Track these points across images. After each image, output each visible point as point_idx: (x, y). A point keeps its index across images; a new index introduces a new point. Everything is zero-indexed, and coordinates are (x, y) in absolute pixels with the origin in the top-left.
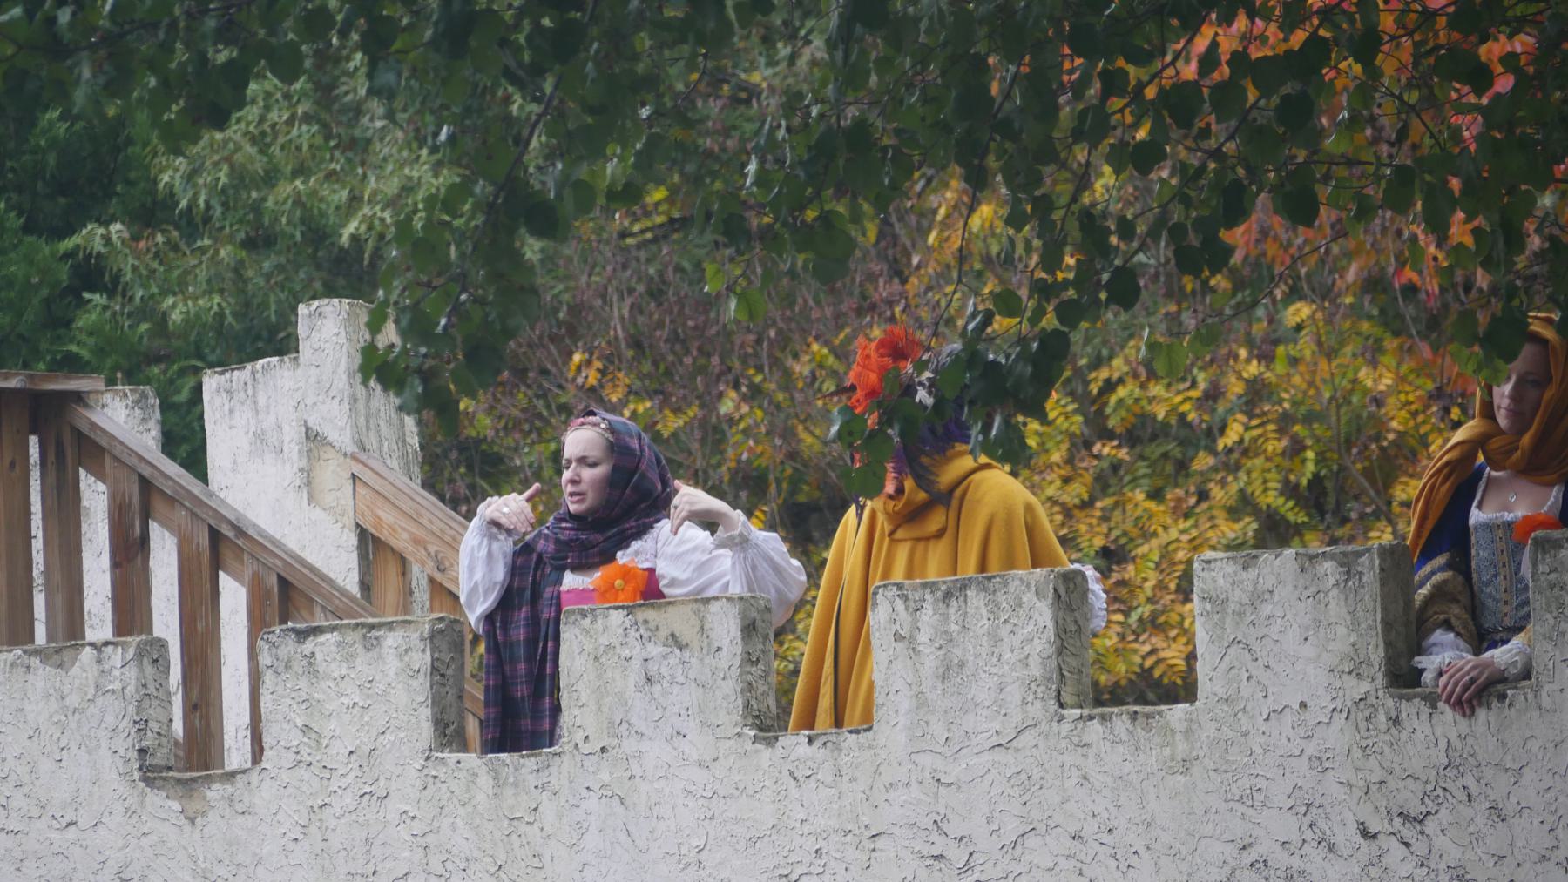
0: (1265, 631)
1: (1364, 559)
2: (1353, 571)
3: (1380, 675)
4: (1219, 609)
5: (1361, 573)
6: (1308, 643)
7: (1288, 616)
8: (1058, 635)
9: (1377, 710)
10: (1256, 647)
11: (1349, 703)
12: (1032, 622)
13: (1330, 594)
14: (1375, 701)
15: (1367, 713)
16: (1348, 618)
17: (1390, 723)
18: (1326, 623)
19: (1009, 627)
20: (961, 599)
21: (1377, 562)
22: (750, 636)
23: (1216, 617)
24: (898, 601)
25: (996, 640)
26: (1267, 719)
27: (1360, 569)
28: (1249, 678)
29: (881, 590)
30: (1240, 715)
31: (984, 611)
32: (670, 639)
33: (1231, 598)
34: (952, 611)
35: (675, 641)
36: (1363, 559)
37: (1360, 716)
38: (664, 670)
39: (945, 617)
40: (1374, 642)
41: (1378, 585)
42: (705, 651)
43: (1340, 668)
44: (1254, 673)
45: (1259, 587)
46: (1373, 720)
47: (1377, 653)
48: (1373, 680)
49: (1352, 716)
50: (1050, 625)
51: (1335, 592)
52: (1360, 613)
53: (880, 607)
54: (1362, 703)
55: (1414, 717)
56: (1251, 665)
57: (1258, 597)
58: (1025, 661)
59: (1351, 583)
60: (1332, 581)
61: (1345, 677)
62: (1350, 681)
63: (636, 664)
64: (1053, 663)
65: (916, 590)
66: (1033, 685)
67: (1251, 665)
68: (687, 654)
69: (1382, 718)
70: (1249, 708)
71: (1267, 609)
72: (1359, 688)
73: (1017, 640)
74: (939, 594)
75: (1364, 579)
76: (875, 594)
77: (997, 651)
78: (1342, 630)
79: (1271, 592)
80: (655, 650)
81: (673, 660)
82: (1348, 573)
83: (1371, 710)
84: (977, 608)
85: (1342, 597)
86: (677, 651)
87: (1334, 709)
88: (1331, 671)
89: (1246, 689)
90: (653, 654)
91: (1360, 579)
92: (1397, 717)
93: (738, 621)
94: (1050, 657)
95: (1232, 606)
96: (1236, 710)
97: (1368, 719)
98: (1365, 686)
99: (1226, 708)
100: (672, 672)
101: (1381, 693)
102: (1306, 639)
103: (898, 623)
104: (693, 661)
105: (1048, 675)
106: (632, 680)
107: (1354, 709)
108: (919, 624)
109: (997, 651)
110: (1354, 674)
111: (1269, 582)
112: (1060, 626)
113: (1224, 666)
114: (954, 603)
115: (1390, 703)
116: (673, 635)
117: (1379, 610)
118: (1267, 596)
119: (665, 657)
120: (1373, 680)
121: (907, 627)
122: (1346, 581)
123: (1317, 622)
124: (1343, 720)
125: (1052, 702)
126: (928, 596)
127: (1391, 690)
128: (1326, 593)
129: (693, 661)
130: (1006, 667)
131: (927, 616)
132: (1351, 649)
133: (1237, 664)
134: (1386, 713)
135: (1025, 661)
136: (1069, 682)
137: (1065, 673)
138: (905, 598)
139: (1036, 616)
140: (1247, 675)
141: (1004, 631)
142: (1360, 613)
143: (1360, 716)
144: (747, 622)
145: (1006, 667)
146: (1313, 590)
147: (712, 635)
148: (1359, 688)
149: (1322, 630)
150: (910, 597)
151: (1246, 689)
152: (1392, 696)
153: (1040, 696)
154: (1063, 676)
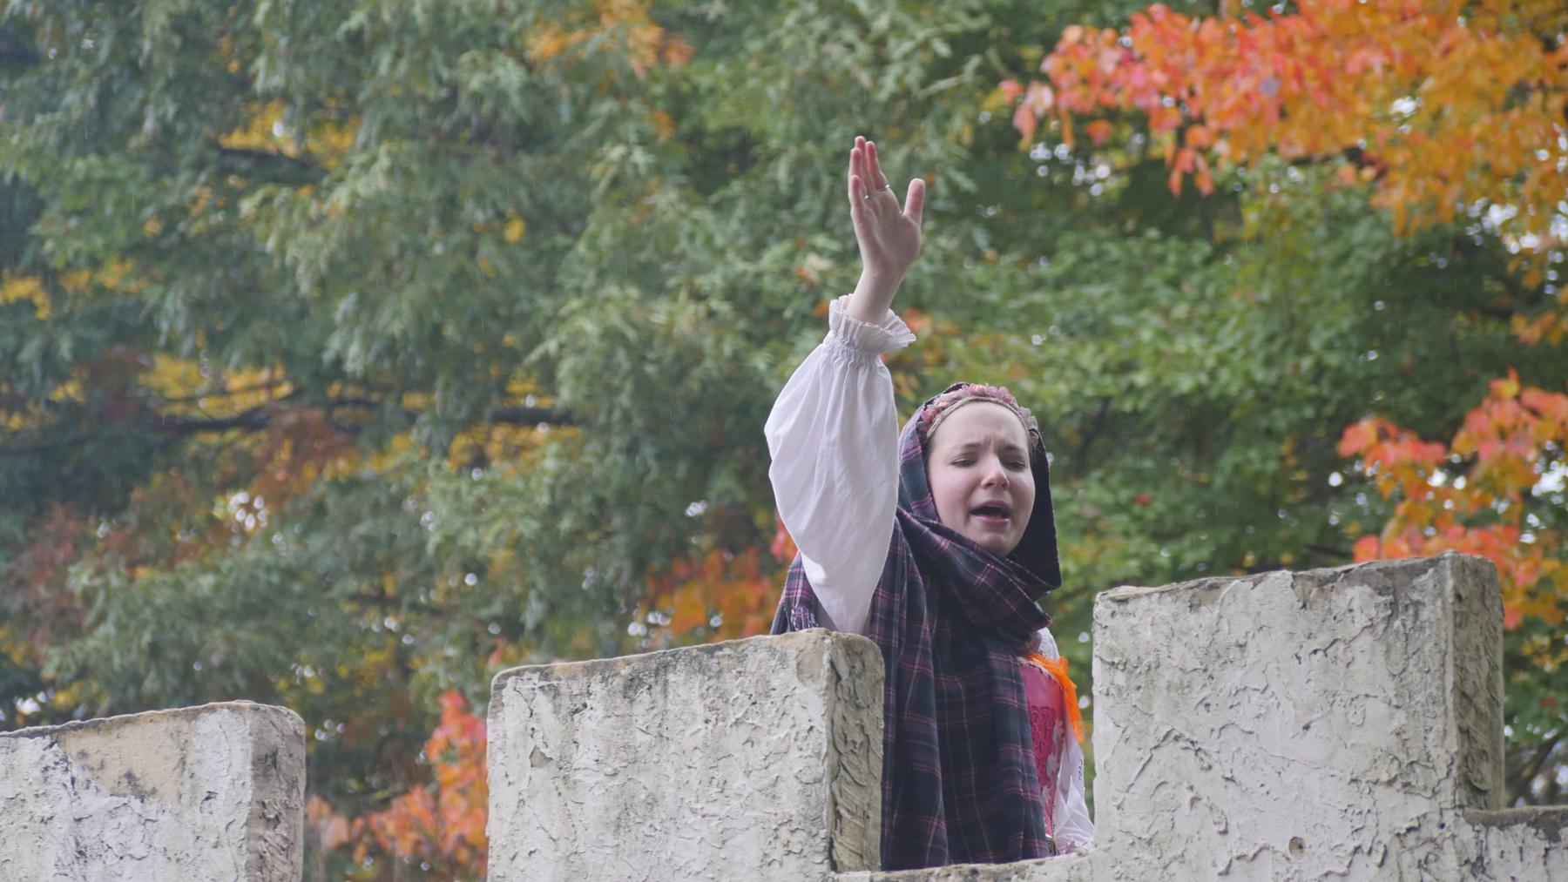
0: (1230, 715)
1: (1427, 579)
2: (1403, 601)
3: (1448, 785)
4: (1141, 681)
5: (1417, 604)
6: (1312, 731)
7: (1273, 688)
8: (833, 744)
9: (1440, 848)
10: (1210, 745)
11: (1386, 838)
12: (787, 721)
13: (1356, 645)
14: (1436, 832)
15: (1421, 854)
16: (1391, 685)
17: (1466, 869)
18: (1346, 697)
19: (743, 732)
20: (658, 688)
21: (1450, 583)
22: (266, 775)
23: (1135, 696)
24: (541, 698)
25: (717, 755)
26: (1226, 872)
27: (1415, 596)
28: (1194, 800)
29: (510, 681)
30: (1174, 867)
31: (699, 708)
32: (125, 782)
33: (1165, 661)
34: (639, 709)
35: (133, 784)
36: (1424, 577)
37: (1407, 858)
38: (110, 837)
39: (627, 721)
40: (1438, 725)
41: (1450, 623)
42: (185, 800)
43: (1372, 776)
44: (1203, 792)
45: (1219, 638)
46: (1433, 866)
47: (1444, 748)
48: (1435, 793)
49: (1391, 861)
50: (821, 725)
51: (1366, 640)
52: (1414, 676)
53: (507, 709)
54: (1412, 835)
55: (1514, 856)
56: (1198, 779)
57: (1215, 658)
58: (770, 792)
59: (1397, 623)
60: (1361, 620)
61: (1380, 791)
62: (1390, 799)
63: (61, 827)
64: (824, 792)
65: (574, 678)
66: (784, 833)
67: (1198, 779)
68: (152, 806)
69: (1450, 860)
70: (1188, 856)
71: (1232, 677)
72: (1402, 810)
73: (756, 755)
74: (618, 682)
75: (1425, 614)
76: (500, 687)
77: (719, 775)
78: (1376, 709)
79: (1242, 646)
80: (95, 802)
81: (126, 819)
82: (1393, 605)
83: (1429, 847)
84: (685, 702)
85: (1381, 648)
86: (136, 803)
87: (1357, 849)
88: (1354, 781)
89: (1186, 821)
90: (90, 811)
91: (1416, 615)
92: (1480, 858)
93: (249, 746)
94: (818, 781)
95: (1167, 675)
96: (1167, 857)
97: (1423, 865)
98: (1419, 806)
99: (1147, 857)
100: (123, 839)
101: (1449, 817)
102: (1307, 727)
103: (538, 735)
104: (162, 818)
105: (812, 813)
106: (50, 857)
107: (1395, 847)
108: (578, 736)
109: (719, 775)
110: (1398, 785)
111: (1240, 628)
112: (837, 729)
113: (1147, 782)
114: (644, 696)
115: (1467, 833)
116: (129, 776)
117: (1450, 668)
118: (1234, 653)
119: (112, 813)
120: (1435, 793)
121: (555, 742)
122: (1389, 620)
123: (1330, 695)
124: (1374, 869)
125: (819, 859)
126: (596, 687)
127: (1471, 811)
128: (1348, 644)
129: (162, 818)
130: (734, 803)
131: (593, 722)
132: (1393, 741)
133: (1172, 778)
134: (1459, 853)
135: (770, 792)
136: (847, 830)
137: (843, 811)
138: (555, 692)
139: (796, 710)
140: (1190, 795)
141: (735, 740)
142: (1414, 676)
143: (1407, 858)
144: (264, 751)
145: (734, 803)
146: (1324, 639)
147: (201, 772)
148: (1402, 810)
149: (1338, 710)
150: (563, 689)
151: (1186, 821)
152: (1471, 821)
153: (796, 849)
154: (838, 815)
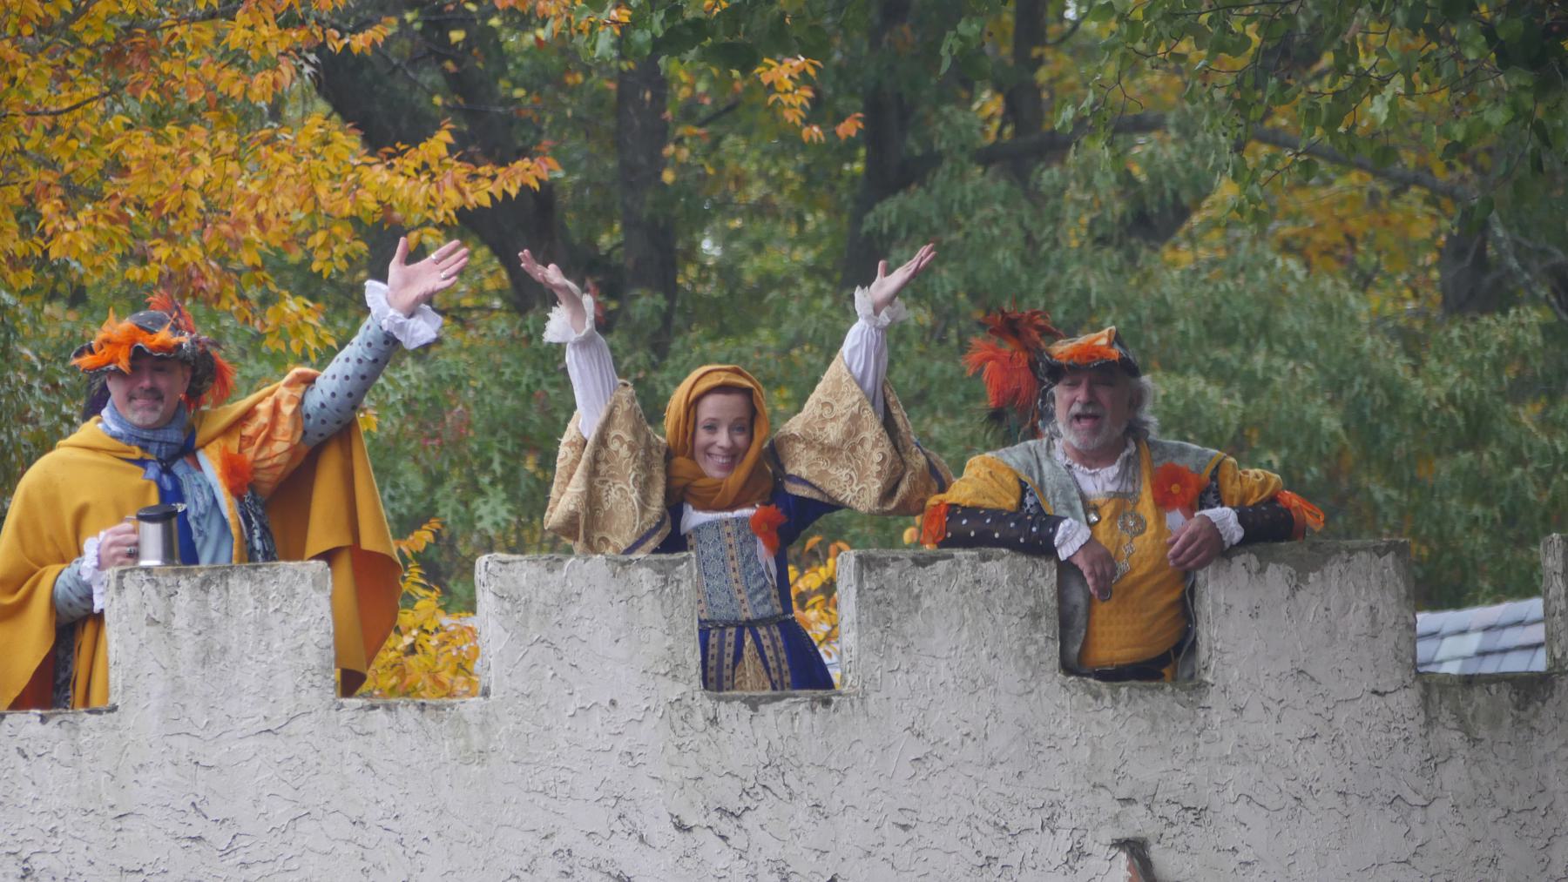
5: (679, 581)
11: (663, 703)
12: (308, 612)
13: (645, 599)
14: (690, 702)
15: (682, 713)
16: (664, 622)
19: (280, 616)
25: (263, 627)
27: (677, 577)
29: (127, 574)
30: (543, 710)
31: (251, 601)
34: (211, 598)
36: (681, 567)
37: (675, 716)
39: (204, 604)
43: (654, 670)
49: (667, 715)
50: (328, 616)
51: (650, 597)
52: (677, 618)
57: (565, 598)
59: (667, 590)
60: (647, 587)
61: (659, 678)
71: (574, 611)
74: (196, 581)
75: (683, 586)
78: (656, 634)
79: (579, 594)
82: (666, 580)
85: (658, 603)
87: (648, 708)
88: (645, 672)
92: (715, 718)
94: (329, 647)
95: (535, 607)
98: (680, 688)
108: (175, 610)
110: (670, 676)
113: (528, 661)
114: (213, 589)
115: (708, 704)
120: (690, 682)
122: (663, 588)
140: (551, 673)
141: (275, 621)
142: (677, 618)
143: (675, 716)
